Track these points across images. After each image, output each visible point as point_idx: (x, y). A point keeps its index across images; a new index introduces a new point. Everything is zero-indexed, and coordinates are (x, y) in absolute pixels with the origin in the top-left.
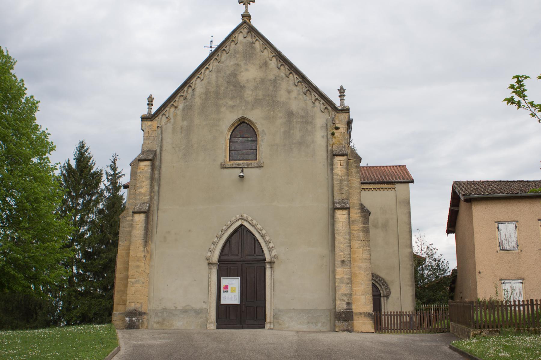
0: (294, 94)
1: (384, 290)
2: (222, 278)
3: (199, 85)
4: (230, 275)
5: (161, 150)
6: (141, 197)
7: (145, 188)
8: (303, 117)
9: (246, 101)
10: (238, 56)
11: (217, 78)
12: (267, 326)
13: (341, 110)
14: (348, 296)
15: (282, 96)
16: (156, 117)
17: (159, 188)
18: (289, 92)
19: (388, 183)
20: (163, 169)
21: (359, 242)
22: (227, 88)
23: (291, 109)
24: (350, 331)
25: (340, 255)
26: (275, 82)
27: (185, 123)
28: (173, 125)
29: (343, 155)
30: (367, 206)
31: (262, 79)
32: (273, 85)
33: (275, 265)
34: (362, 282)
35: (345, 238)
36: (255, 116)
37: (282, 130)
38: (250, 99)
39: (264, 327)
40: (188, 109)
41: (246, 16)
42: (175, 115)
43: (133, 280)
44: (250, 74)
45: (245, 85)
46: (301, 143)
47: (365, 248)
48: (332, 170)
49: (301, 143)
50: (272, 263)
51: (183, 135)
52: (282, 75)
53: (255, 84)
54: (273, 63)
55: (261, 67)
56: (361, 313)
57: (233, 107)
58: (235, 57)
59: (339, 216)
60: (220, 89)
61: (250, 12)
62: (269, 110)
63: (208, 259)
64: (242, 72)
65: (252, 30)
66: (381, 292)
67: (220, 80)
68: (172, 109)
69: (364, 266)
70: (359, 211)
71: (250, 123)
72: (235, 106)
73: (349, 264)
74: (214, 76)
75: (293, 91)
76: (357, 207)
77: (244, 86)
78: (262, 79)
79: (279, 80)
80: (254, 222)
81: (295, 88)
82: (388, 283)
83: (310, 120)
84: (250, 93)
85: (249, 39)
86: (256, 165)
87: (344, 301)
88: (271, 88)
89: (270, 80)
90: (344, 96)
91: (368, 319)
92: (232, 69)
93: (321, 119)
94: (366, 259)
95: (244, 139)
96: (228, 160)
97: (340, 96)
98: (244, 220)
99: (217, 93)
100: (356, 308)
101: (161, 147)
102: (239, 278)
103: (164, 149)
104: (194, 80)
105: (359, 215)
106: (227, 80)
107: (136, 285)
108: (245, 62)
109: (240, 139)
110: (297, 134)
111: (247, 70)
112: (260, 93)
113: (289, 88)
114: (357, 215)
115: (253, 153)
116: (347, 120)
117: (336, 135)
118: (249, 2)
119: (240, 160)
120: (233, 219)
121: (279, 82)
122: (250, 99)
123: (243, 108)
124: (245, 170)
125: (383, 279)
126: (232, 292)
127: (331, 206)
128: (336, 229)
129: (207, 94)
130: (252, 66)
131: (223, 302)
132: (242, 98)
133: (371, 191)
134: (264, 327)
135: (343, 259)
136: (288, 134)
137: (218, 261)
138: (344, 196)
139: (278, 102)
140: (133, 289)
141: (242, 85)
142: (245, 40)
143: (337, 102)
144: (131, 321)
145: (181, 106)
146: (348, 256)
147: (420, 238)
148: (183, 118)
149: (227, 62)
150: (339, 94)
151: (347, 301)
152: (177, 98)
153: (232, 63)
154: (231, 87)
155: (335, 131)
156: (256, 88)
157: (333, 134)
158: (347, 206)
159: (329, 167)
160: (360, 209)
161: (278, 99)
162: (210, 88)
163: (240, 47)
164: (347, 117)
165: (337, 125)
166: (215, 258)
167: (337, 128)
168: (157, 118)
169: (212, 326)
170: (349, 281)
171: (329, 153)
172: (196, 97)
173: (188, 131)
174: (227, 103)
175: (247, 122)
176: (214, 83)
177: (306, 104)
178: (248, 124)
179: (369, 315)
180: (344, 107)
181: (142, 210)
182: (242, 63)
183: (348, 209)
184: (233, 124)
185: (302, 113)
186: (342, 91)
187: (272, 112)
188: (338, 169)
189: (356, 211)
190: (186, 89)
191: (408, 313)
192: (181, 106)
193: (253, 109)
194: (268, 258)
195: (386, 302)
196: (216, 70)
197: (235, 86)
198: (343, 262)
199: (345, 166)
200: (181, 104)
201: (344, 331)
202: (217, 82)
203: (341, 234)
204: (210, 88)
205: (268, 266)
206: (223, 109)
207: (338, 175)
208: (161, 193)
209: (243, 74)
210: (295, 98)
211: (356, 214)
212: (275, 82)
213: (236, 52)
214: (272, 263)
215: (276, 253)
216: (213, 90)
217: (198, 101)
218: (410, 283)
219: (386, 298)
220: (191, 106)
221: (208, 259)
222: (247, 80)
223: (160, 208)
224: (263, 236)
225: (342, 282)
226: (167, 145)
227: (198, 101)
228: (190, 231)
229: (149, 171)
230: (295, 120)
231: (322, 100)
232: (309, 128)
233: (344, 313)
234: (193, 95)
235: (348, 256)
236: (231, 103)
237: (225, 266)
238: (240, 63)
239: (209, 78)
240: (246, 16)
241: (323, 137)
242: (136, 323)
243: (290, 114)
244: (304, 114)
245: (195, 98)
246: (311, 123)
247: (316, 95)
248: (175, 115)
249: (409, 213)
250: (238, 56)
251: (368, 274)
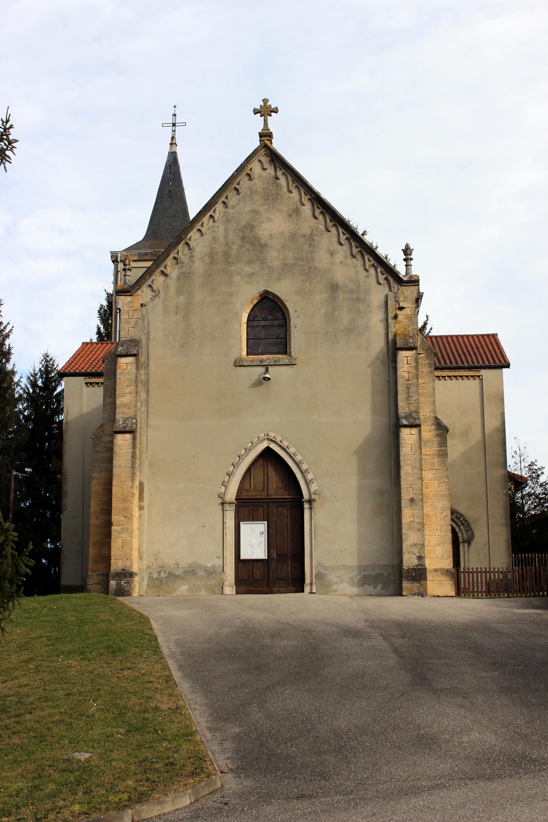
1: (464, 532)
2: (241, 523)
4: (253, 518)
5: (148, 339)
6: (124, 410)
7: (128, 395)
8: (352, 291)
9: (269, 267)
10: (256, 198)
11: (226, 231)
12: (307, 589)
13: (408, 282)
14: (419, 547)
15: (322, 259)
16: (138, 289)
19: (470, 368)
20: (152, 367)
21: (433, 472)
22: (241, 247)
23: (335, 279)
24: (423, 594)
25: (408, 491)
26: (311, 239)
27: (182, 299)
28: (164, 301)
29: (411, 349)
30: (445, 421)
31: (292, 234)
32: (308, 243)
33: (315, 505)
34: (438, 527)
35: (413, 468)
36: (283, 290)
37: (323, 311)
38: (276, 263)
39: (303, 591)
40: (185, 277)
41: (266, 135)
42: (166, 287)
43: (119, 528)
44: (274, 225)
45: (268, 243)
46: (350, 330)
47: (442, 480)
48: (395, 369)
49: (350, 330)
50: (310, 501)
51: (179, 316)
53: (282, 241)
54: (307, 209)
55: (290, 216)
56: (436, 570)
57: (251, 275)
58: (252, 199)
59: (406, 437)
60: (230, 248)
61: (272, 128)
62: (303, 281)
64: (263, 222)
65: (276, 159)
66: (460, 535)
67: (231, 235)
69: (440, 505)
70: (433, 427)
71: (275, 300)
72: (254, 274)
73: (420, 504)
74: (221, 229)
75: (337, 252)
76: (431, 422)
77: (266, 244)
78: (292, 234)
79: (317, 235)
81: (340, 247)
82: (470, 521)
83: (362, 296)
84: (275, 254)
85: (271, 171)
86: (286, 361)
87: (415, 554)
88: (306, 247)
89: (304, 236)
90: (411, 259)
91: (447, 578)
92: (248, 218)
93: (377, 293)
94: (443, 495)
95: (268, 323)
96: (245, 354)
97: (405, 260)
98: (271, 440)
99: (227, 255)
100: (429, 564)
101: (148, 334)
102: (266, 522)
103: (151, 337)
105: (433, 433)
106: (241, 234)
107: (123, 535)
108: (266, 206)
109: (262, 323)
110: (345, 317)
111: (270, 220)
112: (290, 256)
113: (332, 248)
114: (431, 434)
115: (282, 345)
116: (415, 295)
117: (400, 318)
118: (269, 113)
119: (262, 354)
121: (317, 238)
122: (276, 263)
123: (266, 277)
124: (270, 368)
125: (462, 515)
126: (255, 541)
127: (393, 421)
128: (402, 454)
129: (212, 255)
130: (278, 214)
131: (243, 556)
132: (263, 262)
134: (303, 591)
135: (412, 495)
136: (331, 317)
137: (236, 499)
138: (412, 408)
139: (316, 268)
140: (119, 541)
141: (263, 242)
142: (264, 173)
143: (401, 269)
146: (419, 492)
147: (518, 452)
148: (178, 291)
150: (404, 257)
151: (418, 554)
153: (247, 209)
154: (248, 246)
155: (398, 312)
156: (284, 247)
157: (396, 317)
158: (417, 422)
159: (391, 366)
160: (434, 424)
161: (317, 265)
162: (216, 246)
163: (257, 183)
164: (416, 292)
165: (402, 304)
166: (231, 494)
167: (401, 309)
168: (139, 291)
169: (230, 590)
170: (420, 527)
171: (390, 344)
172: (195, 259)
173: (186, 311)
174: (242, 270)
175: (271, 297)
176: (222, 239)
177: (357, 272)
178: (272, 300)
179: (447, 572)
180: (411, 277)
181: (128, 429)
182: (262, 209)
183: (418, 426)
185: (351, 286)
186: (407, 251)
187: (308, 284)
188: (405, 369)
189: (429, 428)
191: (501, 570)
193: (280, 279)
194: (306, 495)
195: (466, 549)
196: (224, 219)
197: (252, 244)
198: (412, 500)
199: (414, 364)
201: (415, 595)
202: (226, 237)
203: (409, 462)
204: (216, 246)
205: (306, 506)
206: (237, 279)
207: (404, 377)
208: (150, 402)
209: (264, 225)
210: (341, 262)
211: (428, 431)
212: (311, 239)
213: (252, 192)
215: (317, 488)
216: (220, 249)
217: (199, 267)
218: (503, 521)
219: (466, 545)
220: (190, 273)
222: (271, 235)
223: (149, 424)
224: (298, 465)
225: (411, 528)
226: (156, 332)
227: (199, 267)
228: (194, 456)
229: (134, 371)
230: (341, 296)
231: (379, 266)
232: (362, 307)
233: (414, 569)
234: (192, 256)
235: (419, 492)
236: (248, 269)
237: (247, 507)
238: (259, 208)
239: (214, 231)
240: (266, 135)
241: (381, 321)
242: (127, 588)
243: (334, 288)
244: (354, 288)
245: (194, 262)
246: (364, 300)
247: (371, 259)
248: (166, 287)
249: (503, 415)
250: (256, 198)
251: (445, 516)
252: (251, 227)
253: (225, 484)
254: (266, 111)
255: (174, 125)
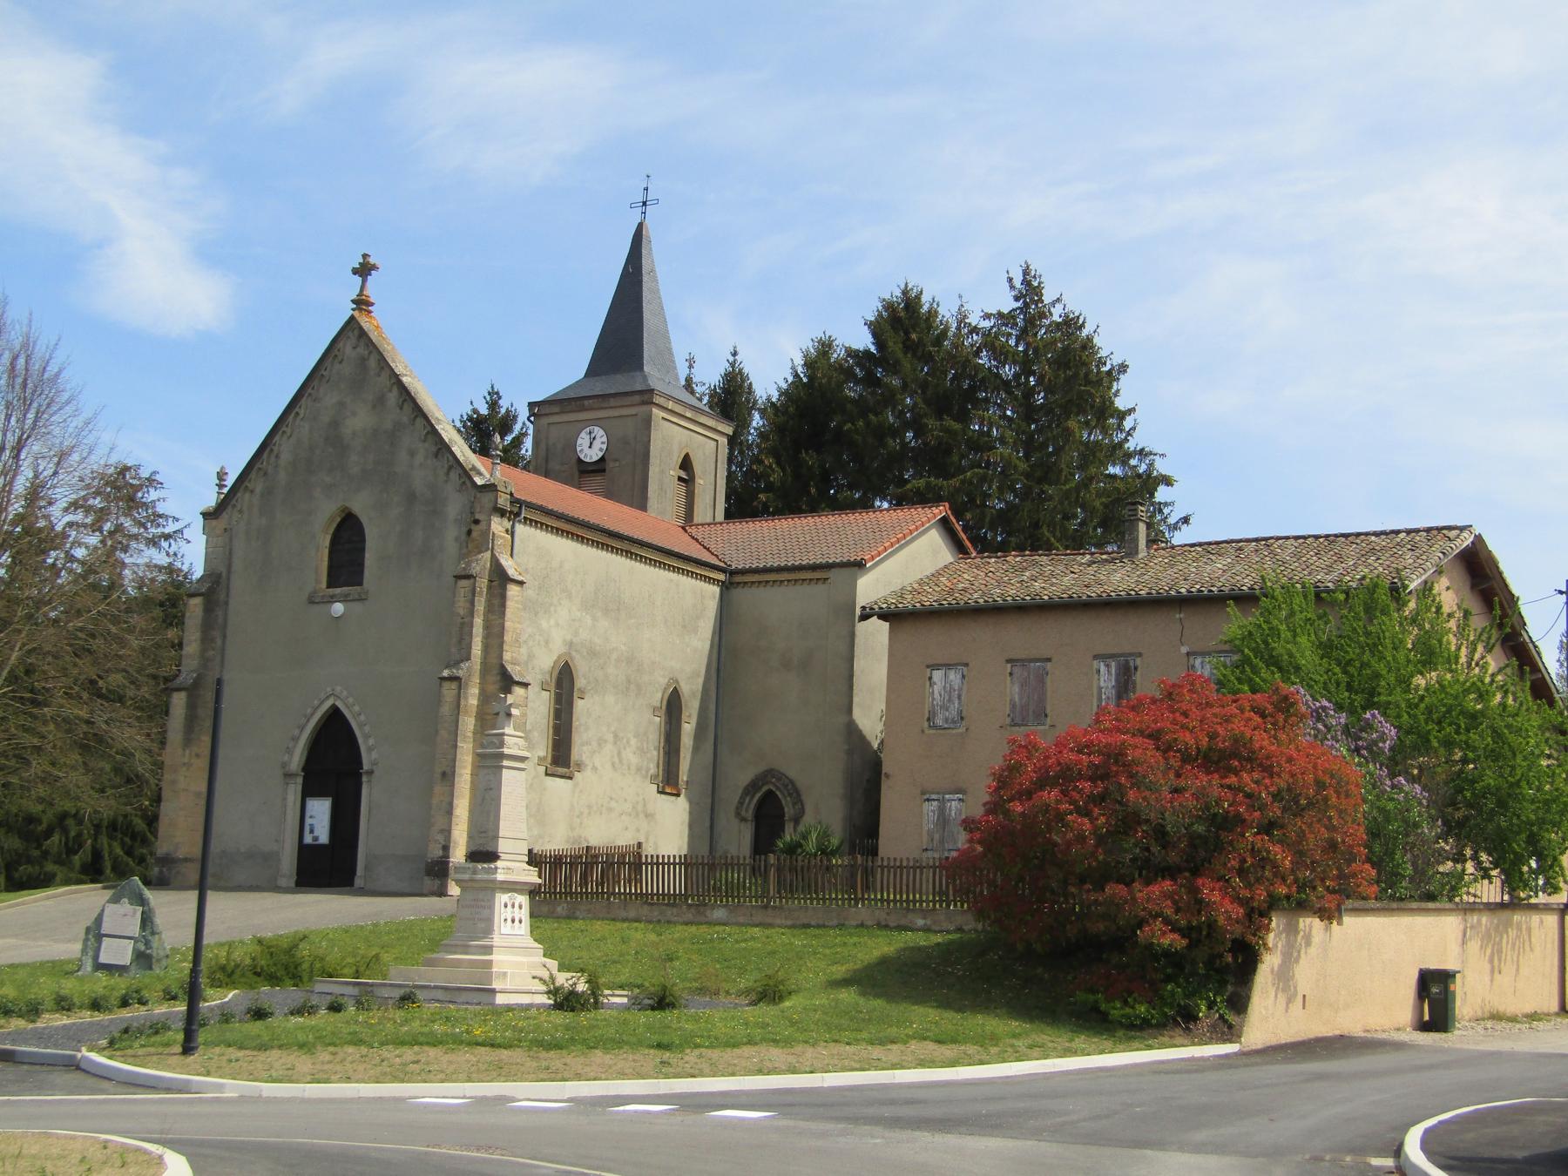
0: (420, 458)
3: (285, 449)
5: (229, 572)
17: (224, 642)
18: (412, 454)
20: (233, 603)
36: (360, 506)
41: (362, 303)
44: (359, 421)
50: (370, 773)
52: (405, 419)
55: (374, 407)
61: (372, 292)
63: (284, 765)
68: (247, 495)
80: (351, 700)
101: (229, 567)
104: (277, 438)
111: (354, 414)
117: (474, 534)
120: (323, 696)
125: (792, 782)
133: (783, 589)
144: (161, 872)
145: (258, 489)
149: (329, 398)
152: (253, 475)
155: (474, 527)
184: (332, 519)
190: (265, 455)
192: (258, 489)
200: (257, 484)
205: (364, 779)
214: (370, 773)
217: (282, 476)
221: (284, 765)
222: (354, 434)
226: (238, 564)
227: (282, 476)
240: (362, 303)
243: (411, 497)
252: (335, 424)
253: (289, 751)
254: (364, 270)
255: (644, 204)
